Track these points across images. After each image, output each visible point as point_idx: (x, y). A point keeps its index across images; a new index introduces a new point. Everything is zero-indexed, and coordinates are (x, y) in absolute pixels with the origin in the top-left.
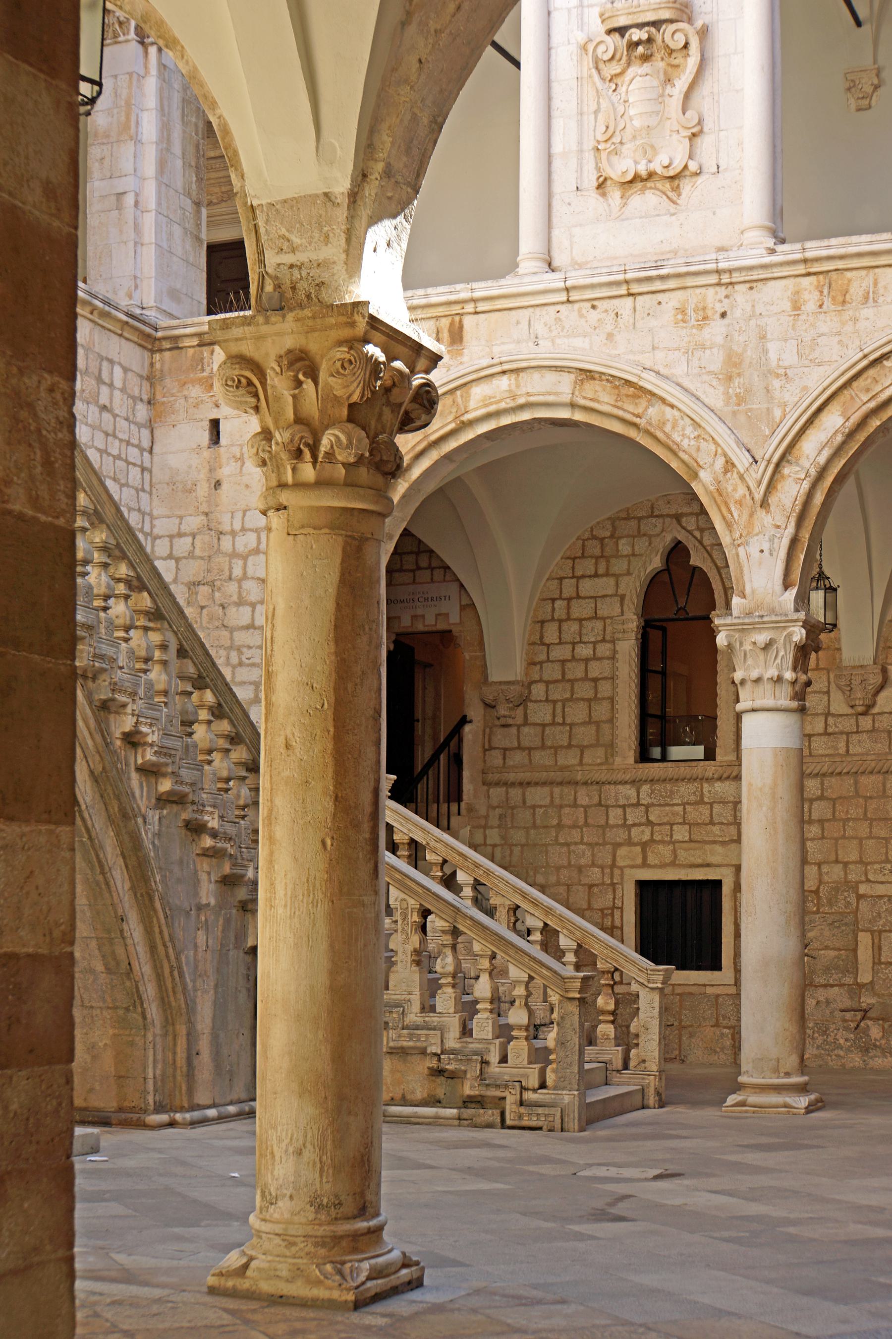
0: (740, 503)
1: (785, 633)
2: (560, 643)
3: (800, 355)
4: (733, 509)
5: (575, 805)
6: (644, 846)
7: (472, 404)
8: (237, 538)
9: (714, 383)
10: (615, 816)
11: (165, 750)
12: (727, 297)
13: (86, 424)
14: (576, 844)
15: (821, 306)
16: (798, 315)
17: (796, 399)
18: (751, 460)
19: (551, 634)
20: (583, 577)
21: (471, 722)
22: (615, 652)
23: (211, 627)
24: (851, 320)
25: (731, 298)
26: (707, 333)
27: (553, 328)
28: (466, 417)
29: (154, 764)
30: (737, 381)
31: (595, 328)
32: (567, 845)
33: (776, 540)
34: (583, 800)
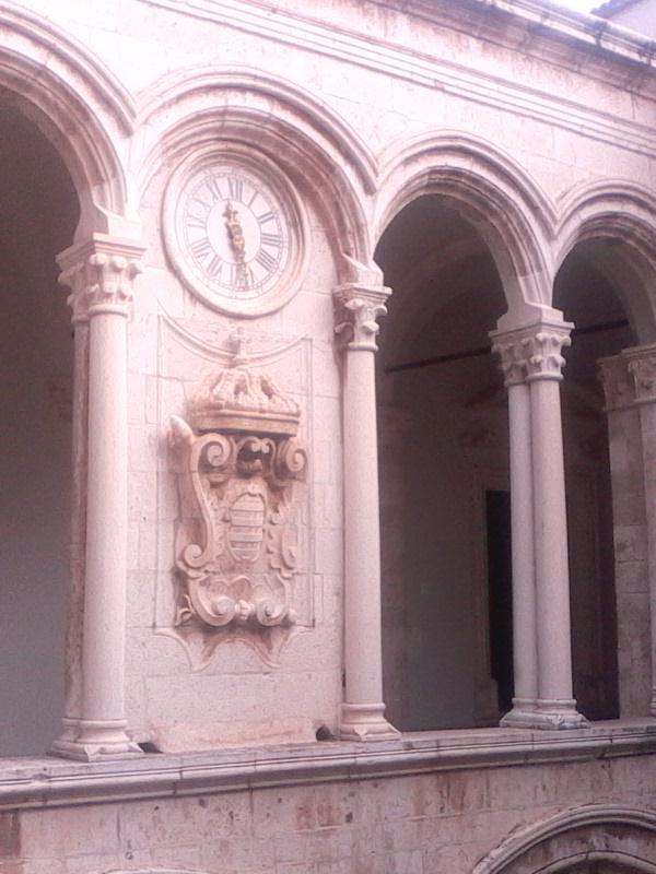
12: (352, 795)
15: (442, 809)
16: (422, 820)
26: (332, 841)
31: (206, 834)
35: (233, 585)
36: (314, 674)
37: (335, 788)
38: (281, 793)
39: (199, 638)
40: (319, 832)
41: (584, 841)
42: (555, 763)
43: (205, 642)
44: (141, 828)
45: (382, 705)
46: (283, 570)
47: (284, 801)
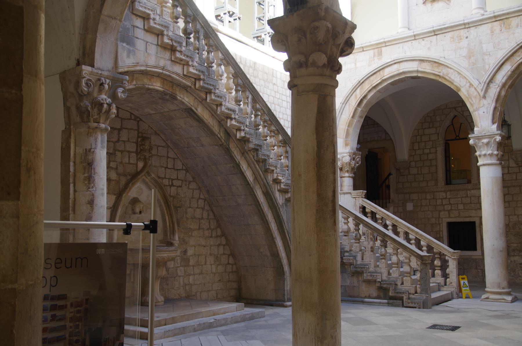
0: (475, 97)
1: (494, 139)
2: (419, 149)
3: (494, 47)
4: (473, 99)
5: (426, 199)
6: (449, 211)
10: (439, 202)
11: (287, 184)
13: (269, 89)
14: (427, 211)
15: (501, 31)
16: (493, 34)
18: (479, 83)
19: (416, 146)
20: (425, 128)
21: (392, 174)
22: (436, 151)
24: (512, 34)
25: (469, 32)
29: (284, 189)
30: (472, 58)
32: (424, 211)
33: (489, 108)
34: (428, 197)
37: (462, 31)
43: (431, 5)
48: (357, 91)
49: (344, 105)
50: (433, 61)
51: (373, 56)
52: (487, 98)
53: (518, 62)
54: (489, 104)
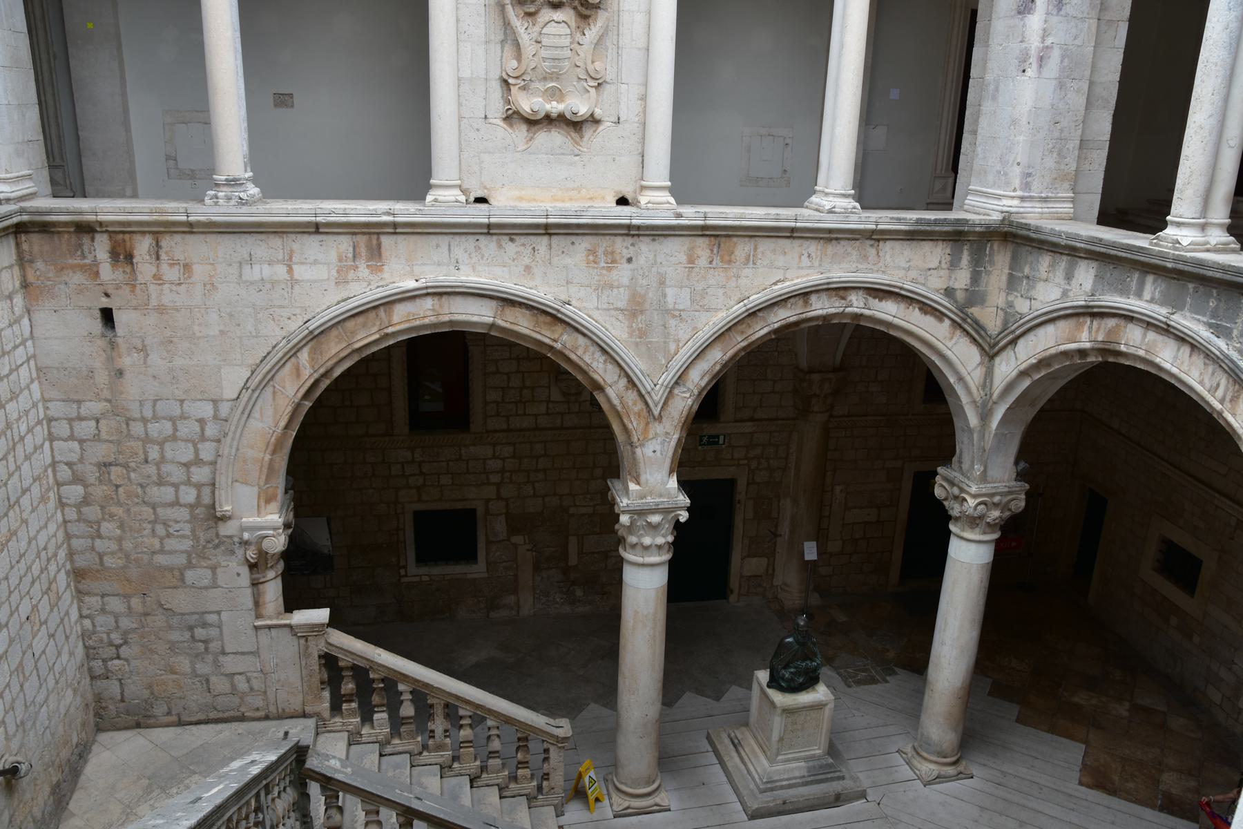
1: (673, 514)
3: (692, 301)
7: (396, 319)
8: (149, 425)
9: (620, 318)
12: (633, 245)
15: (711, 262)
16: (692, 268)
17: (688, 337)
23: (130, 502)
25: (636, 246)
26: (614, 274)
27: (473, 255)
28: (390, 330)
31: (514, 260)
33: (666, 444)
35: (546, 90)
36: (617, 158)
37: (619, 239)
38: (573, 238)
39: (524, 127)
40: (604, 267)
41: (843, 298)
42: (821, 238)
44: (466, 252)
45: (669, 183)
46: (589, 79)
47: (577, 244)
48: (299, 354)
49: (256, 395)
50: (538, 309)
51: (351, 255)
52: (664, 419)
53: (739, 346)
54: (667, 433)
